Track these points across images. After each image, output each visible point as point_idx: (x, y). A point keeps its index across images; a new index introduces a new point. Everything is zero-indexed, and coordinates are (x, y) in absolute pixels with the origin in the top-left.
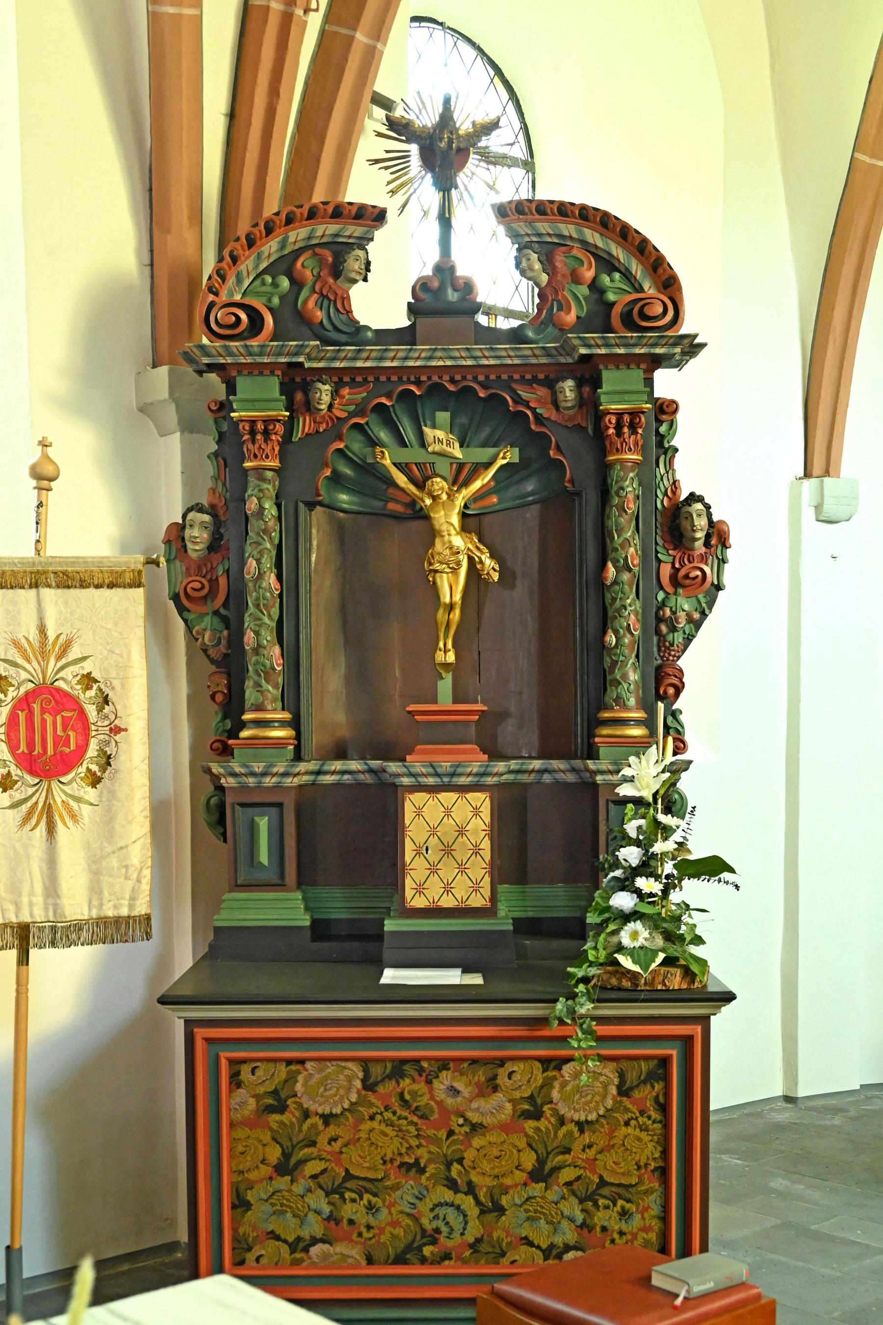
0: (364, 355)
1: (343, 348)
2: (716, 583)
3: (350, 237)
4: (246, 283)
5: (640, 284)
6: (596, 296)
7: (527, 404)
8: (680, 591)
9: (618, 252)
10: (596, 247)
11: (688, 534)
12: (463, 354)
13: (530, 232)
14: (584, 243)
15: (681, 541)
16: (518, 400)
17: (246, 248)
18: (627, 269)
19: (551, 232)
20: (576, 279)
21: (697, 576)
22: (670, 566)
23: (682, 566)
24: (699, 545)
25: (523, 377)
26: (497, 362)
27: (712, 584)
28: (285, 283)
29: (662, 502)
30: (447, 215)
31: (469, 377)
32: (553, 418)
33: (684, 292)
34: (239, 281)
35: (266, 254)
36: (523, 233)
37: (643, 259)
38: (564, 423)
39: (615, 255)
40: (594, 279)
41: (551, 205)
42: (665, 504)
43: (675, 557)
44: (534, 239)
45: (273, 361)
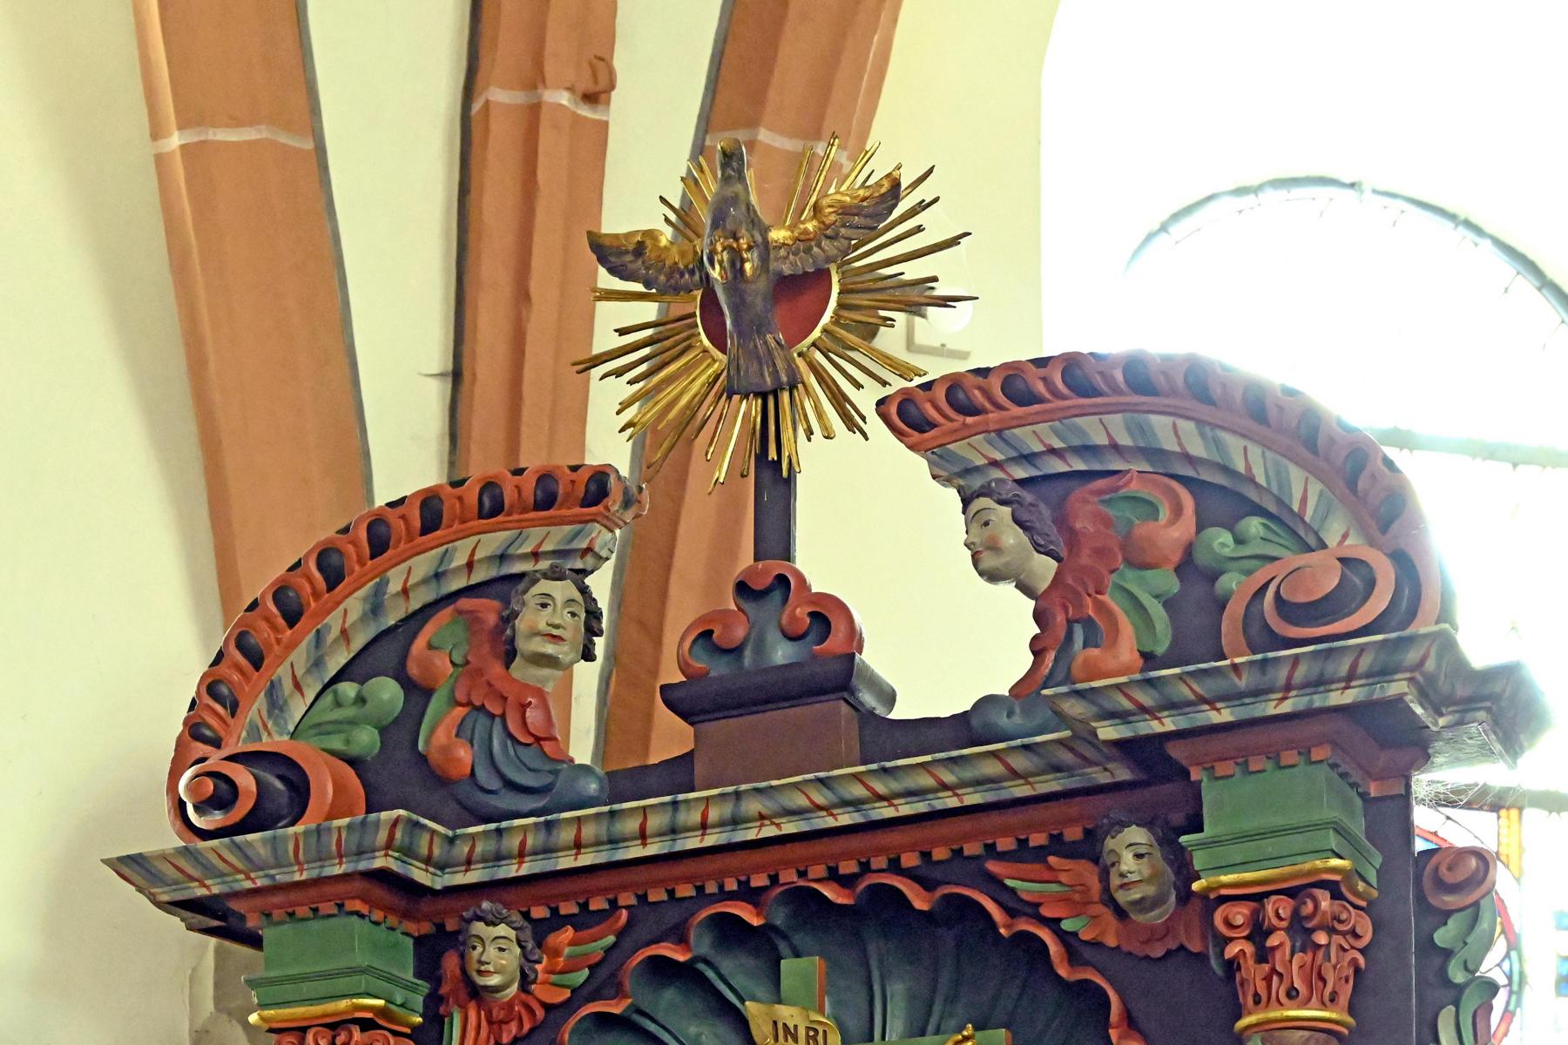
0: (566, 835)
1: (504, 824)
3: (536, 555)
4: (297, 708)
7: (1032, 910)
13: (999, 456)
16: (1015, 906)
17: (281, 621)
25: (1023, 843)
26: (921, 807)
28: (387, 692)
30: (773, 455)
31: (879, 862)
32: (1111, 942)
34: (276, 705)
35: (335, 632)
36: (981, 461)
38: (1139, 951)
45: (314, 874)
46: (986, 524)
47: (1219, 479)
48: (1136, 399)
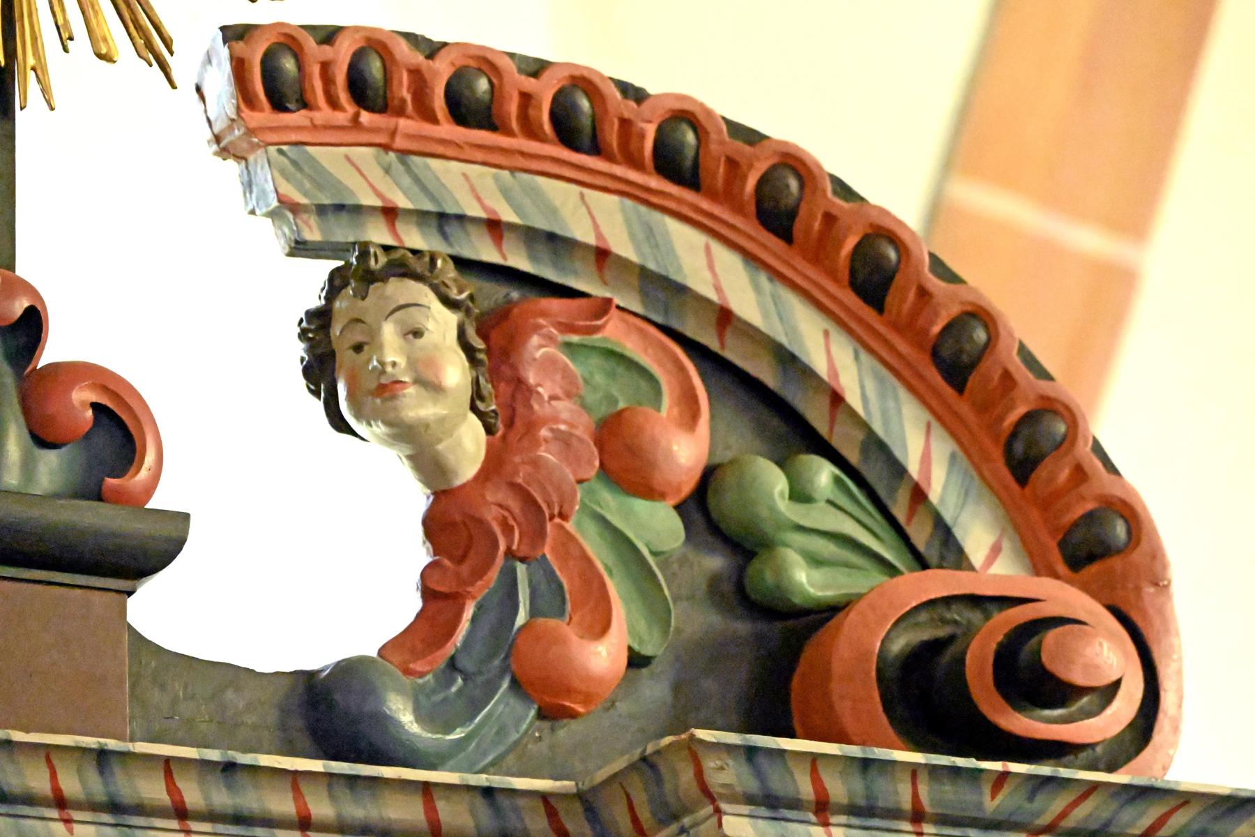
5: (944, 533)
6: (715, 562)
9: (833, 355)
10: (725, 317)
12: (71, 785)
13: (402, 202)
14: (661, 287)
18: (876, 446)
19: (508, 215)
20: (622, 459)
33: (1175, 589)
36: (369, 200)
37: (963, 407)
39: (821, 367)
40: (709, 475)
41: (530, 84)
44: (414, 238)
46: (417, 333)
47: (766, 373)
48: (655, 182)
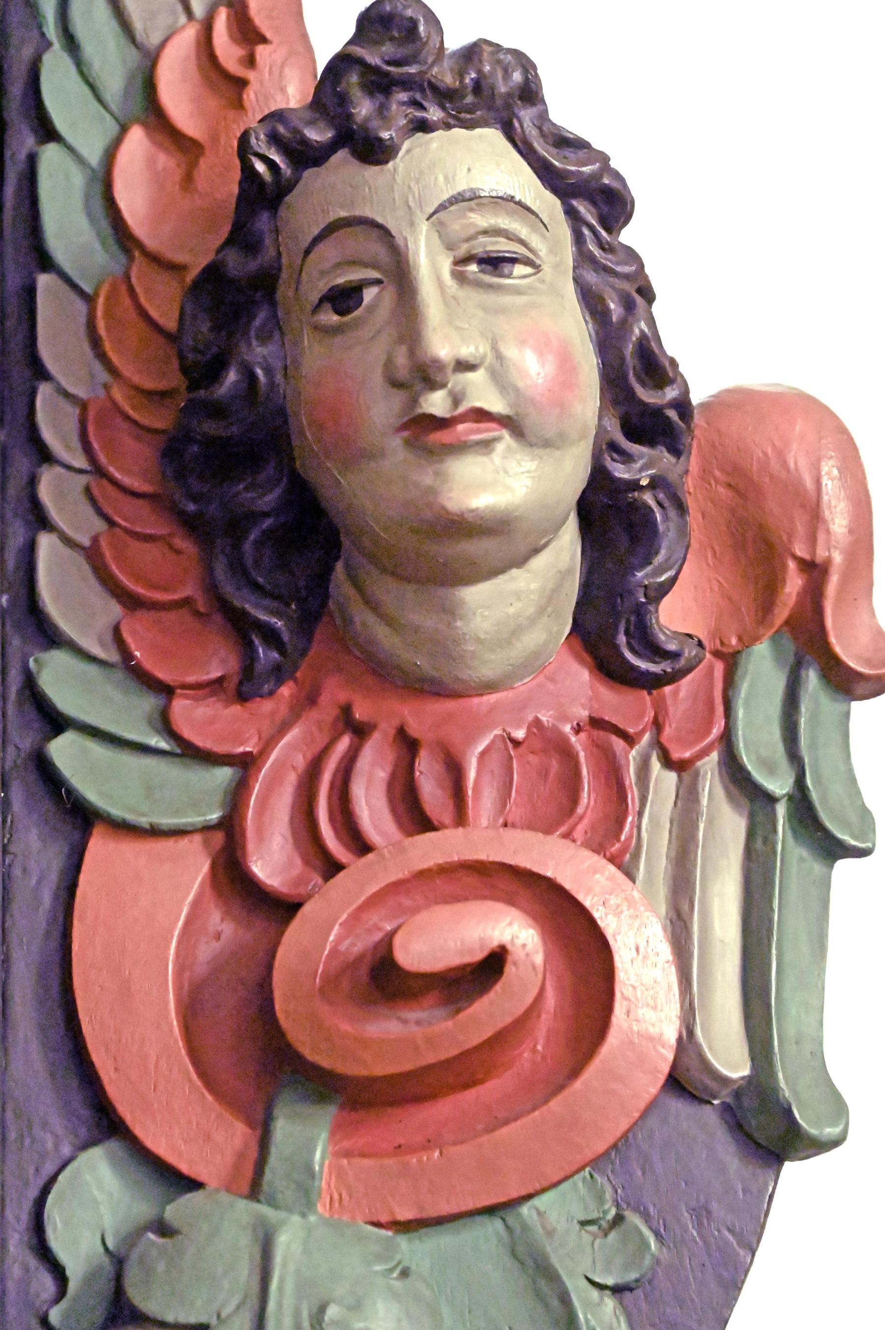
2: (731, 1060)
8: (306, 1136)
11: (372, 488)
15: (312, 607)
21: (495, 962)
22: (195, 866)
23: (332, 868)
24: (517, 613)
27: (685, 1080)
29: (104, 181)
42: (132, 200)
43: (246, 764)
